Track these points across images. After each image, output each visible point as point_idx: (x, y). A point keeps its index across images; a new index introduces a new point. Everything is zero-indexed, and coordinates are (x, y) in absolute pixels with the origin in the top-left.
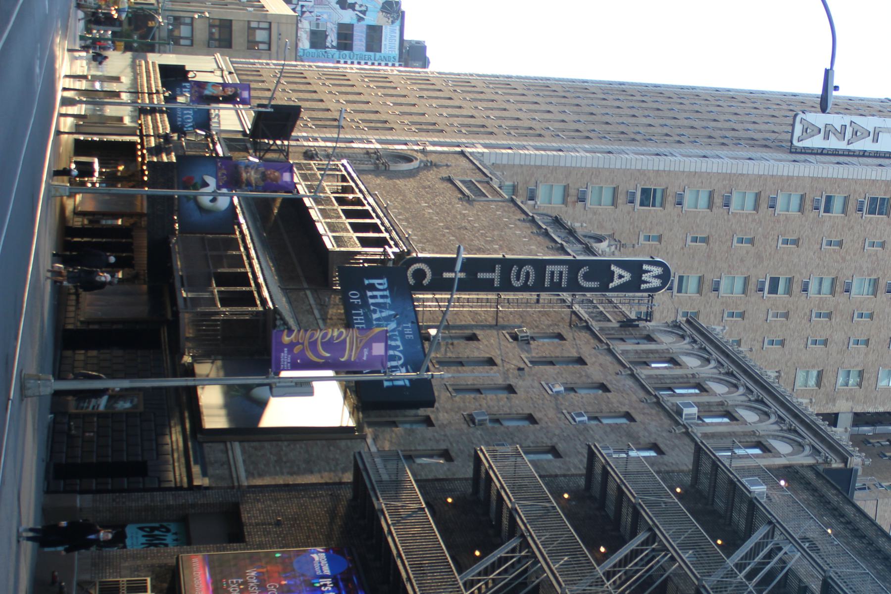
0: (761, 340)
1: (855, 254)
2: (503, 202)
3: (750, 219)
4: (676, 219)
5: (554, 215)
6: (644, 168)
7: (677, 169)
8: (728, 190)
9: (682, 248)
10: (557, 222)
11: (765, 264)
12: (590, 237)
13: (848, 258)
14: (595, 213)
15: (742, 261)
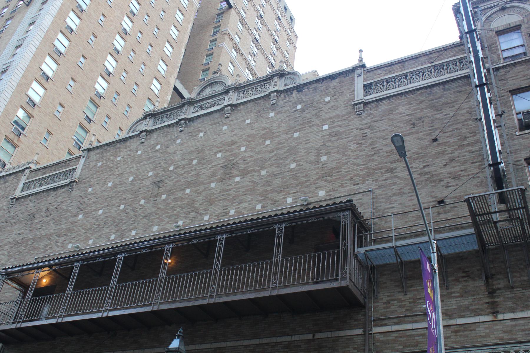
0: (132, 94)
1: (112, 14)
2: (88, 157)
3: (72, 48)
4: (55, 88)
5: (141, 116)
6: (18, 81)
7: (27, 64)
8: (52, 46)
9: (72, 97)
10: (153, 115)
11: (98, 60)
12: (202, 90)
13: (112, 18)
14: (31, 132)
15: (92, 71)
